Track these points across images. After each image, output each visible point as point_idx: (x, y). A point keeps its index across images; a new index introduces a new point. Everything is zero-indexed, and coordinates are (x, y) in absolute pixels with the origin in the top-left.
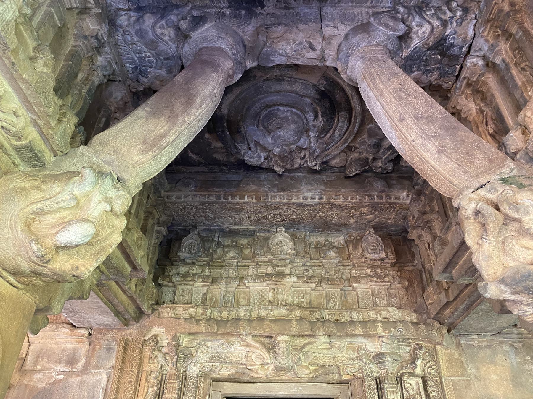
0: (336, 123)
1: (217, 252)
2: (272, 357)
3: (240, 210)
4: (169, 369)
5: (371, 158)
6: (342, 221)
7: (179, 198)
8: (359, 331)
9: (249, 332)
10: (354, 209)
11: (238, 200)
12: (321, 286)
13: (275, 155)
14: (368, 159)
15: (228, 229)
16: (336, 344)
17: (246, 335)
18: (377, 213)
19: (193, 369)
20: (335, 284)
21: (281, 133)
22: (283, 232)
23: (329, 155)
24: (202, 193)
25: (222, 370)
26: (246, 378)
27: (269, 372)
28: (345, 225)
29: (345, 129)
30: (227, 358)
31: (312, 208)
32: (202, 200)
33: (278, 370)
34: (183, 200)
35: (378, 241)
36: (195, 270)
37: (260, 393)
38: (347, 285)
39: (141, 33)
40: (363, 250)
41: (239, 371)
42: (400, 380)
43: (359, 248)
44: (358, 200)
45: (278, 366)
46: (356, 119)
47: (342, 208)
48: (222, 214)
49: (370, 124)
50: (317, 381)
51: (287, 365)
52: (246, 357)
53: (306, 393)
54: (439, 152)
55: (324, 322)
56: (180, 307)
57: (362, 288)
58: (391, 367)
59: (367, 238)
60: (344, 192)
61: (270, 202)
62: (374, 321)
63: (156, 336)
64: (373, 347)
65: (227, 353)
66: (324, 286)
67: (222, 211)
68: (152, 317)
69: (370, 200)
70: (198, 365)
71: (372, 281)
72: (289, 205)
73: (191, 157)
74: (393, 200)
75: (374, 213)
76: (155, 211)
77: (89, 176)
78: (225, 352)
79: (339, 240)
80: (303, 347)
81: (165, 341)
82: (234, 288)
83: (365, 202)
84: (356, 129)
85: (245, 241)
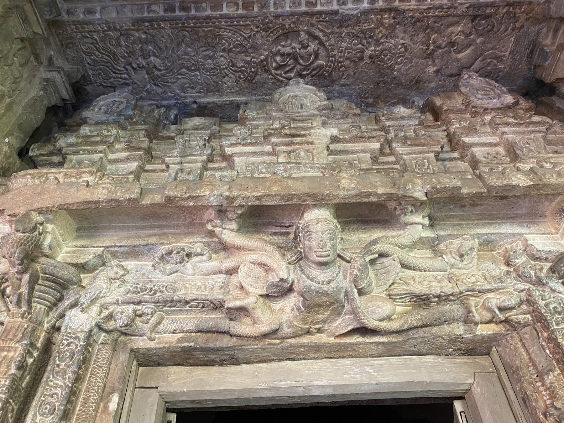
1: (169, 128)
2: (292, 267)
7: (90, 12)
9: (227, 193)
11: (209, 12)
12: (392, 154)
16: (452, 244)
17: (221, 212)
20: (424, 145)
22: (301, 85)
25: (161, 327)
26: (225, 342)
27: (285, 317)
30: (175, 290)
32: (137, 15)
34: (98, 16)
35: (490, 85)
37: (263, 386)
38: (447, 148)
41: (205, 326)
43: (455, 98)
45: (309, 289)
48: (179, 58)
50: (408, 347)
51: (332, 285)
52: (225, 286)
53: (386, 380)
56: (60, 173)
59: (469, 82)
61: (272, 11)
64: (547, 242)
65: (175, 283)
66: (400, 149)
67: (179, 45)
70: (95, 309)
71: (507, 124)
75: (474, 40)
78: (170, 278)
80: (375, 242)
82: (199, 165)
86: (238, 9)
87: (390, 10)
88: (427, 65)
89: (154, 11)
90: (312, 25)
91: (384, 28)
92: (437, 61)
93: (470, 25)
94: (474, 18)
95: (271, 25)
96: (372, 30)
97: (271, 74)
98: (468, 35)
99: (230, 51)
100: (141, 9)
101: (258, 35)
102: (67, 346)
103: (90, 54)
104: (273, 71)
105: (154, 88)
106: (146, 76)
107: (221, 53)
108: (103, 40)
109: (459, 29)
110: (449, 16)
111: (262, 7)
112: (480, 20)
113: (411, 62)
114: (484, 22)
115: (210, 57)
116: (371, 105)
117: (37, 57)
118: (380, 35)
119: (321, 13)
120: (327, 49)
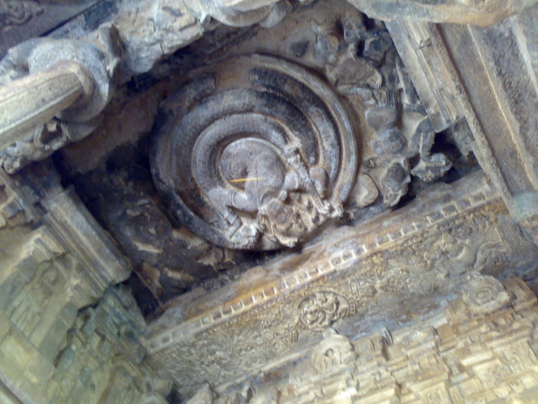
0: (317, 134)
5: (402, 161)
6: (426, 285)
10: (425, 250)
11: (244, 308)
12: (410, 392)
13: (265, 217)
14: (398, 164)
15: (262, 375)
18: (467, 241)
23: (343, 186)
24: (195, 319)
29: (332, 133)
31: (357, 275)
40: (467, 305)
44: (417, 229)
46: (336, 112)
47: (402, 253)
49: (364, 111)
60: (389, 226)
67: (232, 337)
69: (435, 219)
73: (171, 278)
74: (474, 204)
75: (462, 244)
76: (125, 364)
83: (430, 227)
84: (347, 125)
86: (263, 297)
87: (376, 254)
88: (435, 275)
89: (207, 323)
90: (321, 286)
91: (378, 266)
92: (442, 269)
93: (450, 236)
94: (450, 230)
95: (291, 299)
96: (370, 271)
97: (308, 329)
98: (455, 242)
99: (270, 326)
100: (198, 325)
101: (285, 309)
103: (174, 367)
104: (310, 327)
105: (227, 372)
106: (218, 367)
107: (264, 330)
108: (179, 355)
109: (443, 241)
110: (426, 239)
111: (279, 289)
112: (456, 230)
113: (419, 278)
114: (460, 229)
115: (256, 337)
116: (408, 320)
117: (139, 389)
118: (379, 272)
119: (323, 277)
120: (344, 297)
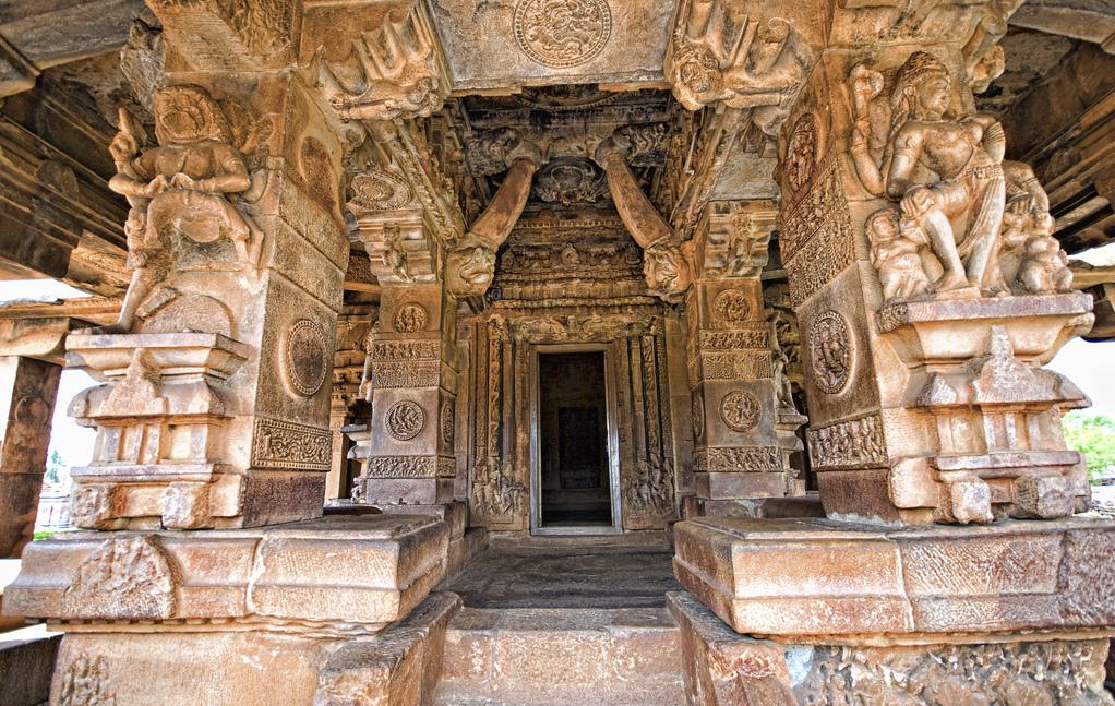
3: (540, 233)
4: (505, 338)
8: (617, 311)
11: (538, 227)
19: (519, 338)
21: (566, 182)
28: (615, 239)
33: (569, 335)
36: (514, 277)
39: (482, 153)
42: (640, 337)
54: (638, 227)
55: (597, 306)
57: (622, 284)
58: (636, 330)
62: (627, 305)
63: (494, 320)
68: (491, 309)
72: (575, 228)
77: (479, 250)
79: (611, 249)
81: (501, 321)
85: (544, 254)
102: (518, 344)
